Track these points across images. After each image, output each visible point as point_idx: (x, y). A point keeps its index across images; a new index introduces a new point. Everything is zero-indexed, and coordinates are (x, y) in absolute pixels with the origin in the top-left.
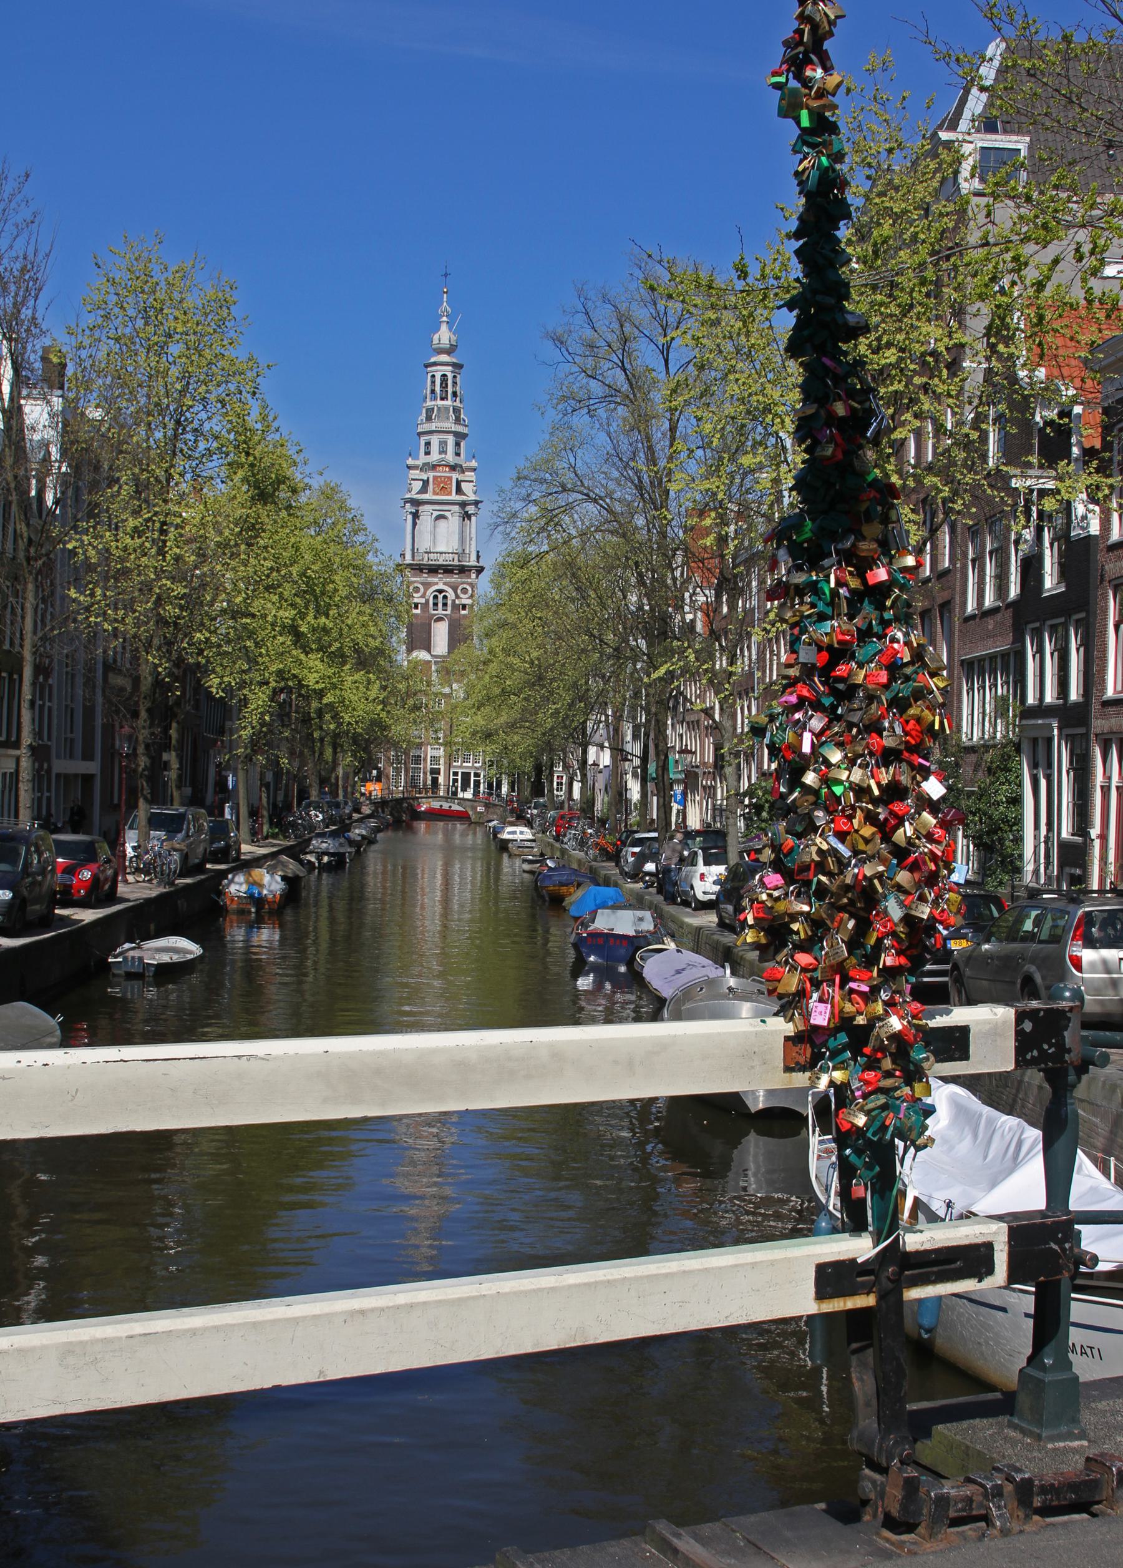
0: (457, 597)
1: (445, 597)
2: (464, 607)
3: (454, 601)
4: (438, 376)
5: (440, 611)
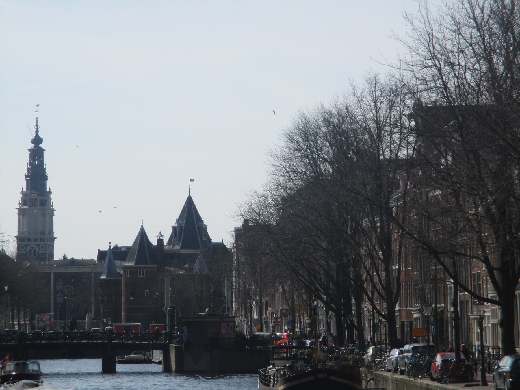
0: (40, 250)
1: (35, 251)
2: (43, 254)
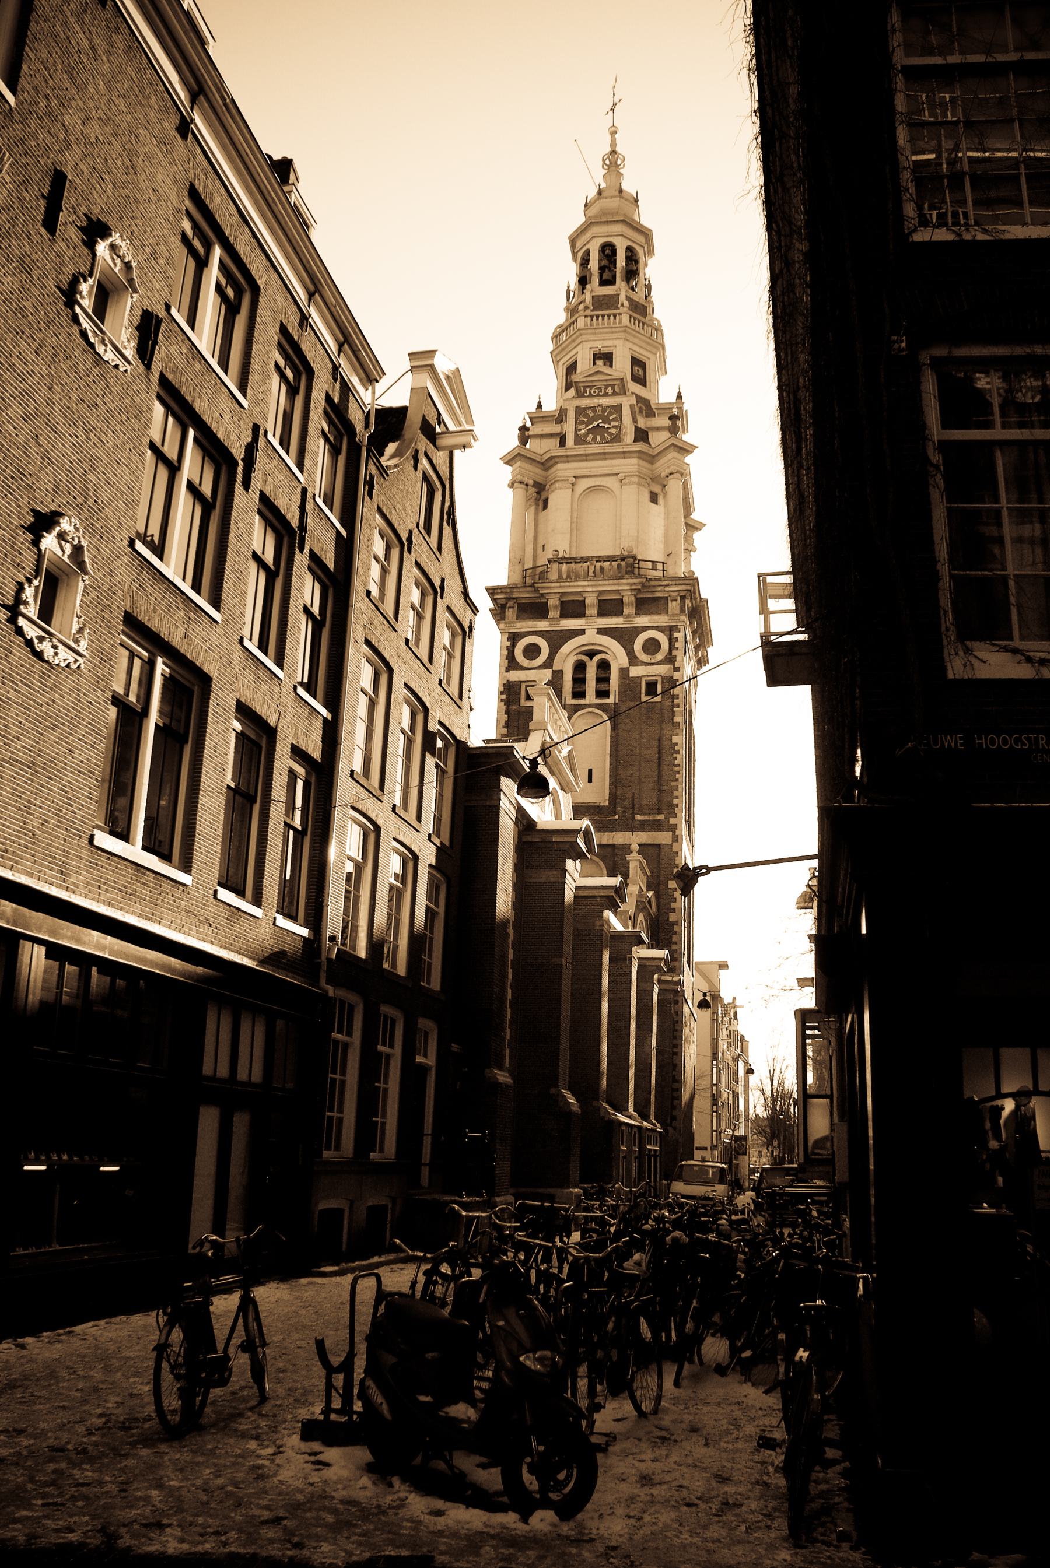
0: (633, 659)
1: (604, 666)
2: (651, 688)
3: (624, 672)
4: (595, 248)
5: (591, 698)
